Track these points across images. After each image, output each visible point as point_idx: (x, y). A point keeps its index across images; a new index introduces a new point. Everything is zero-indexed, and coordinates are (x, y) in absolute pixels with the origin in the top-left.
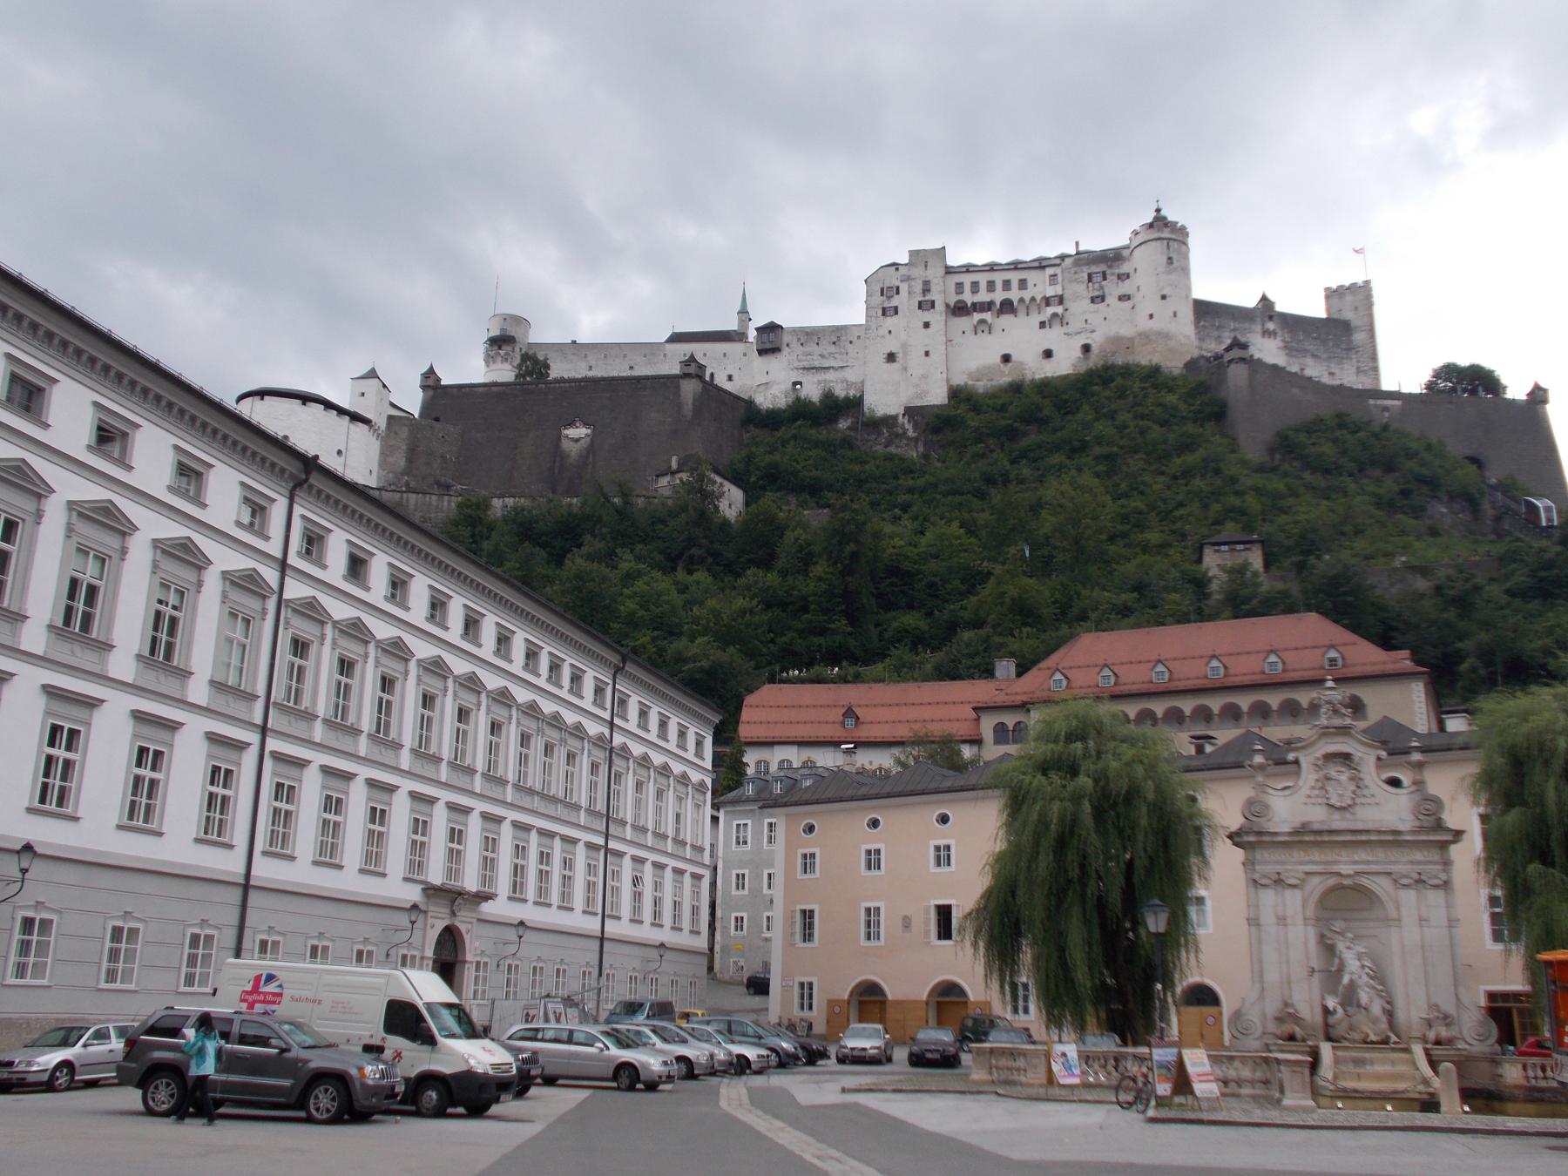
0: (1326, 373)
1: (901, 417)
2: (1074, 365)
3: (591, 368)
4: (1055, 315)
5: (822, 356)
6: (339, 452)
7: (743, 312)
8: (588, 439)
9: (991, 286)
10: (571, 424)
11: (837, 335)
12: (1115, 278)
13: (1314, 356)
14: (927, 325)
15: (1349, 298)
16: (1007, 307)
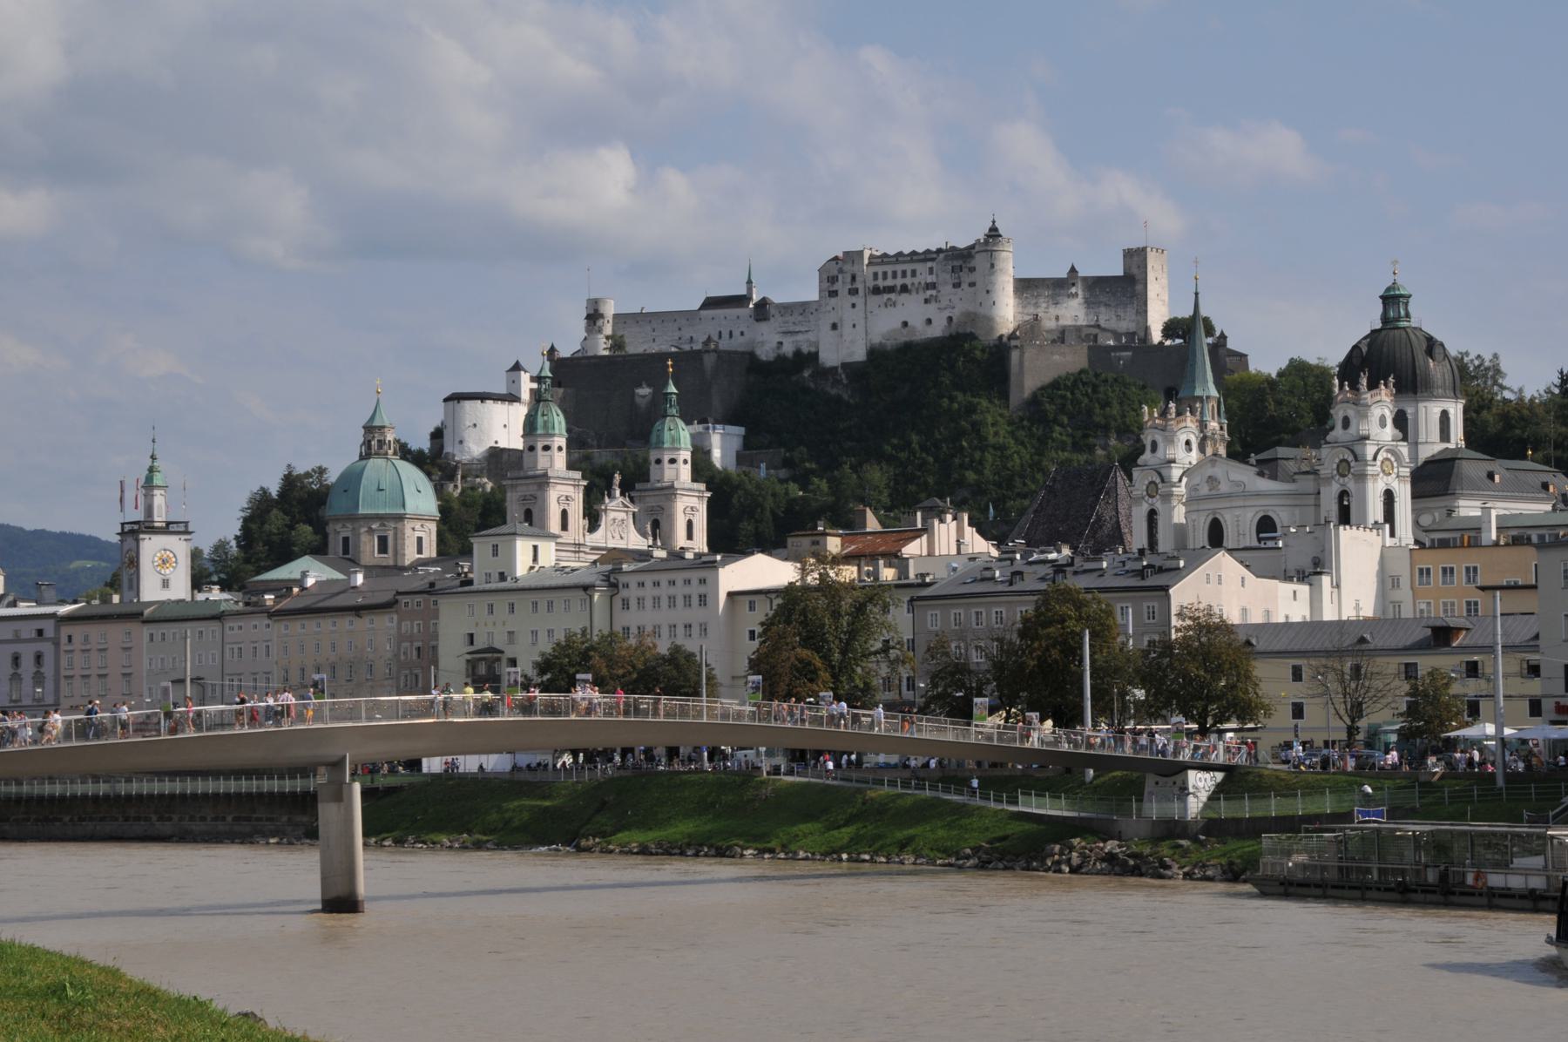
0: (1114, 317)
1: (840, 370)
2: (943, 331)
3: (654, 330)
4: (931, 296)
5: (794, 323)
6: (505, 426)
7: (749, 282)
8: (650, 396)
9: (895, 275)
10: (640, 386)
11: (803, 307)
12: (967, 270)
13: (1107, 305)
14: (854, 306)
15: (1135, 258)
16: (904, 289)
